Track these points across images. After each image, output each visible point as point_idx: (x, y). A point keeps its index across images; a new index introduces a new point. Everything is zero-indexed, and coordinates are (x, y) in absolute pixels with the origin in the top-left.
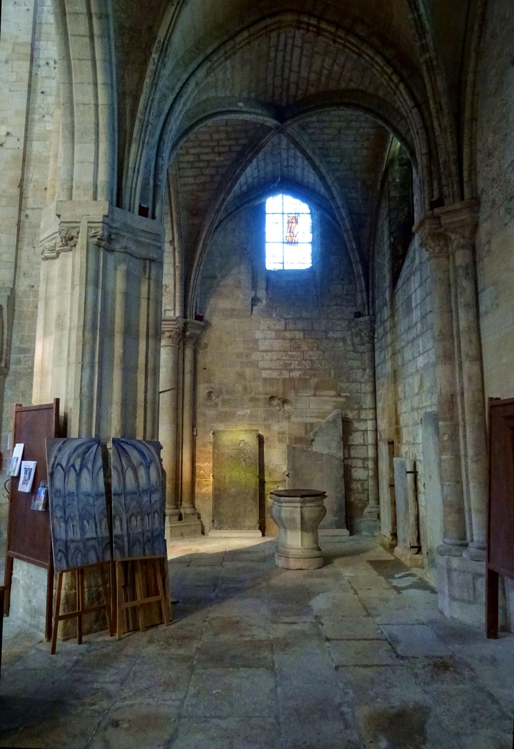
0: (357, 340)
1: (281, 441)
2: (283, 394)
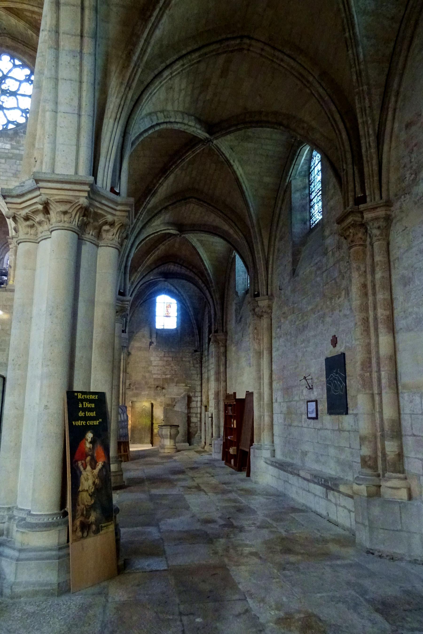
0: (195, 362)
1: (161, 406)
2: (163, 385)
